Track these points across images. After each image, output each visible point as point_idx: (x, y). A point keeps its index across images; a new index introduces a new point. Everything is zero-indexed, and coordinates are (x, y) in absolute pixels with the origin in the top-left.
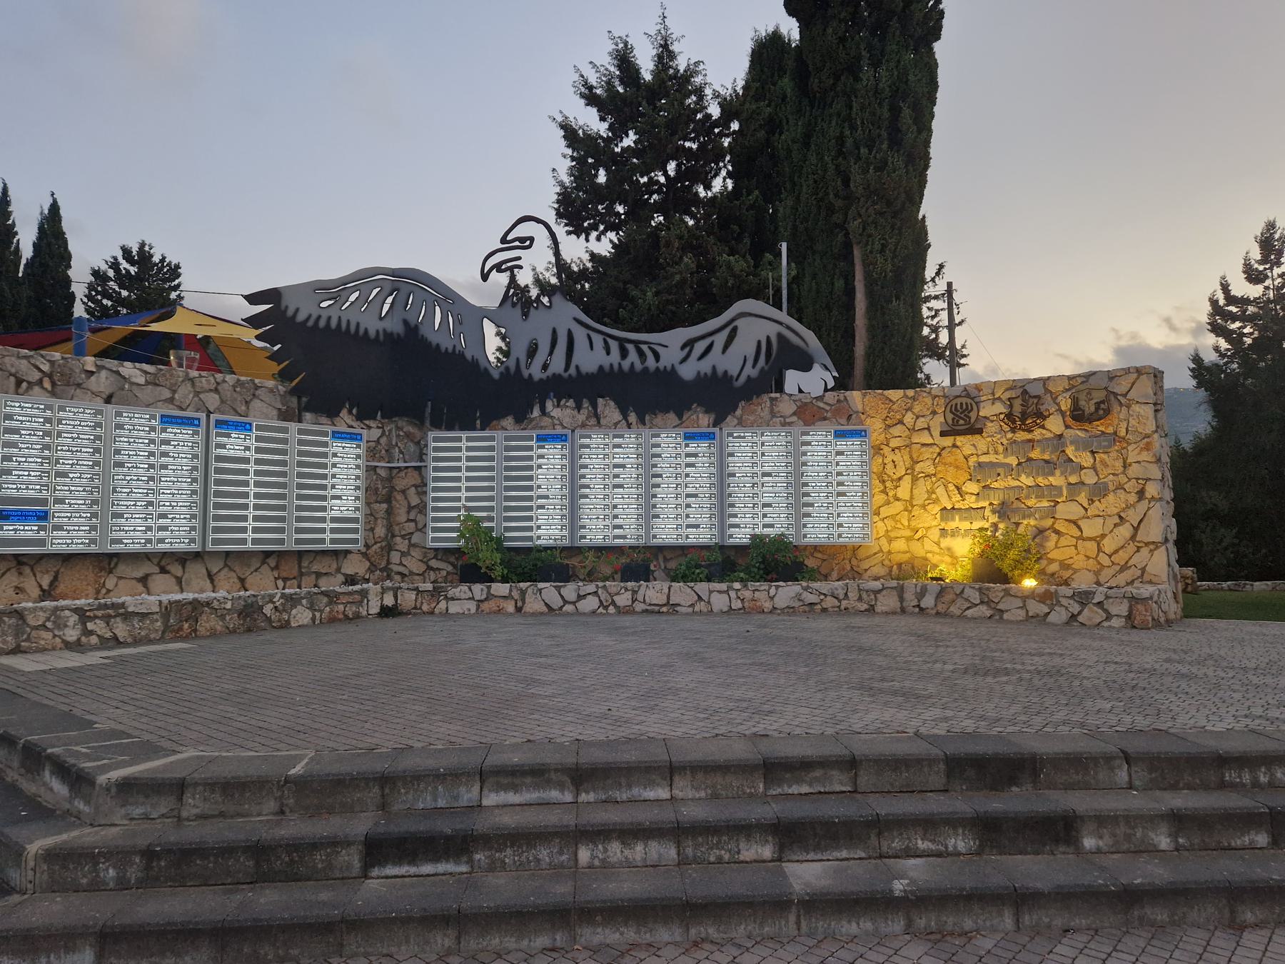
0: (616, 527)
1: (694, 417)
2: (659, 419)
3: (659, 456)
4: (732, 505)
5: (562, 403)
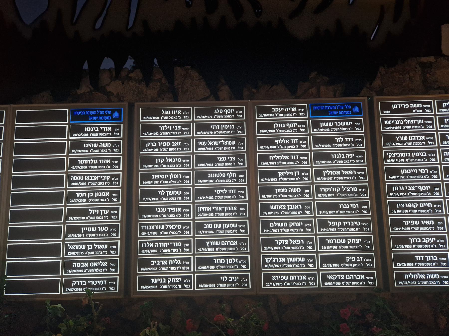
0: (201, 262)
3: (271, 142)
4: (399, 223)
5: (123, 74)
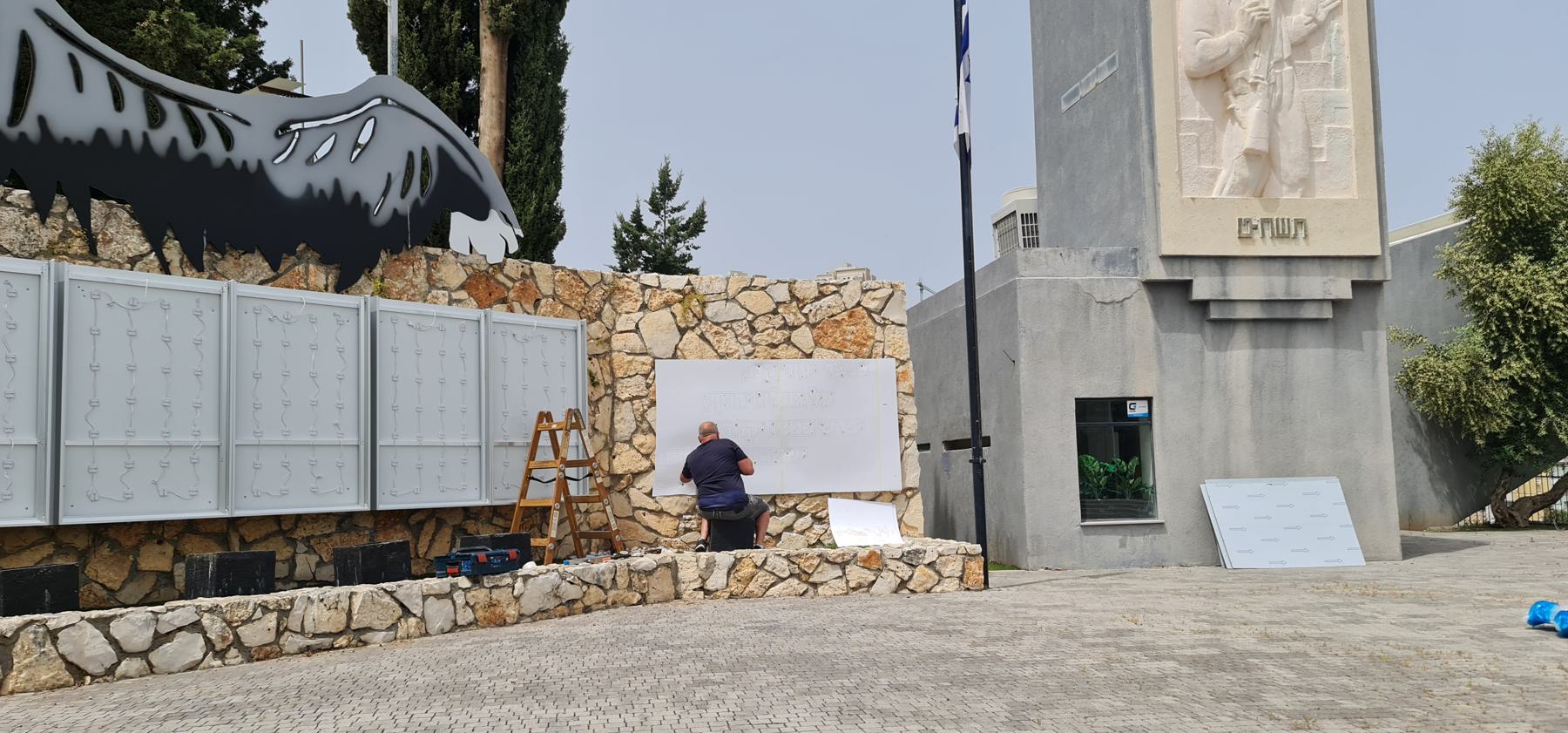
1: (301, 268)
2: (227, 265)
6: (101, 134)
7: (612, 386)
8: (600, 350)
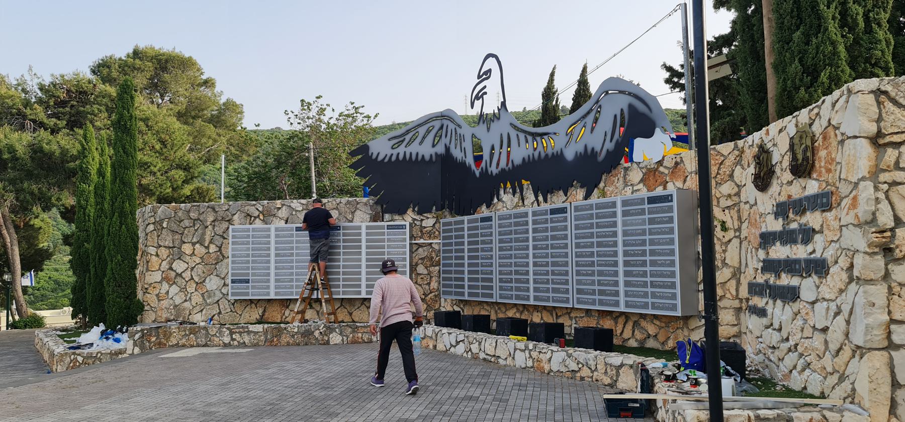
6: (524, 159)
7: (739, 230)
8: (729, 203)
